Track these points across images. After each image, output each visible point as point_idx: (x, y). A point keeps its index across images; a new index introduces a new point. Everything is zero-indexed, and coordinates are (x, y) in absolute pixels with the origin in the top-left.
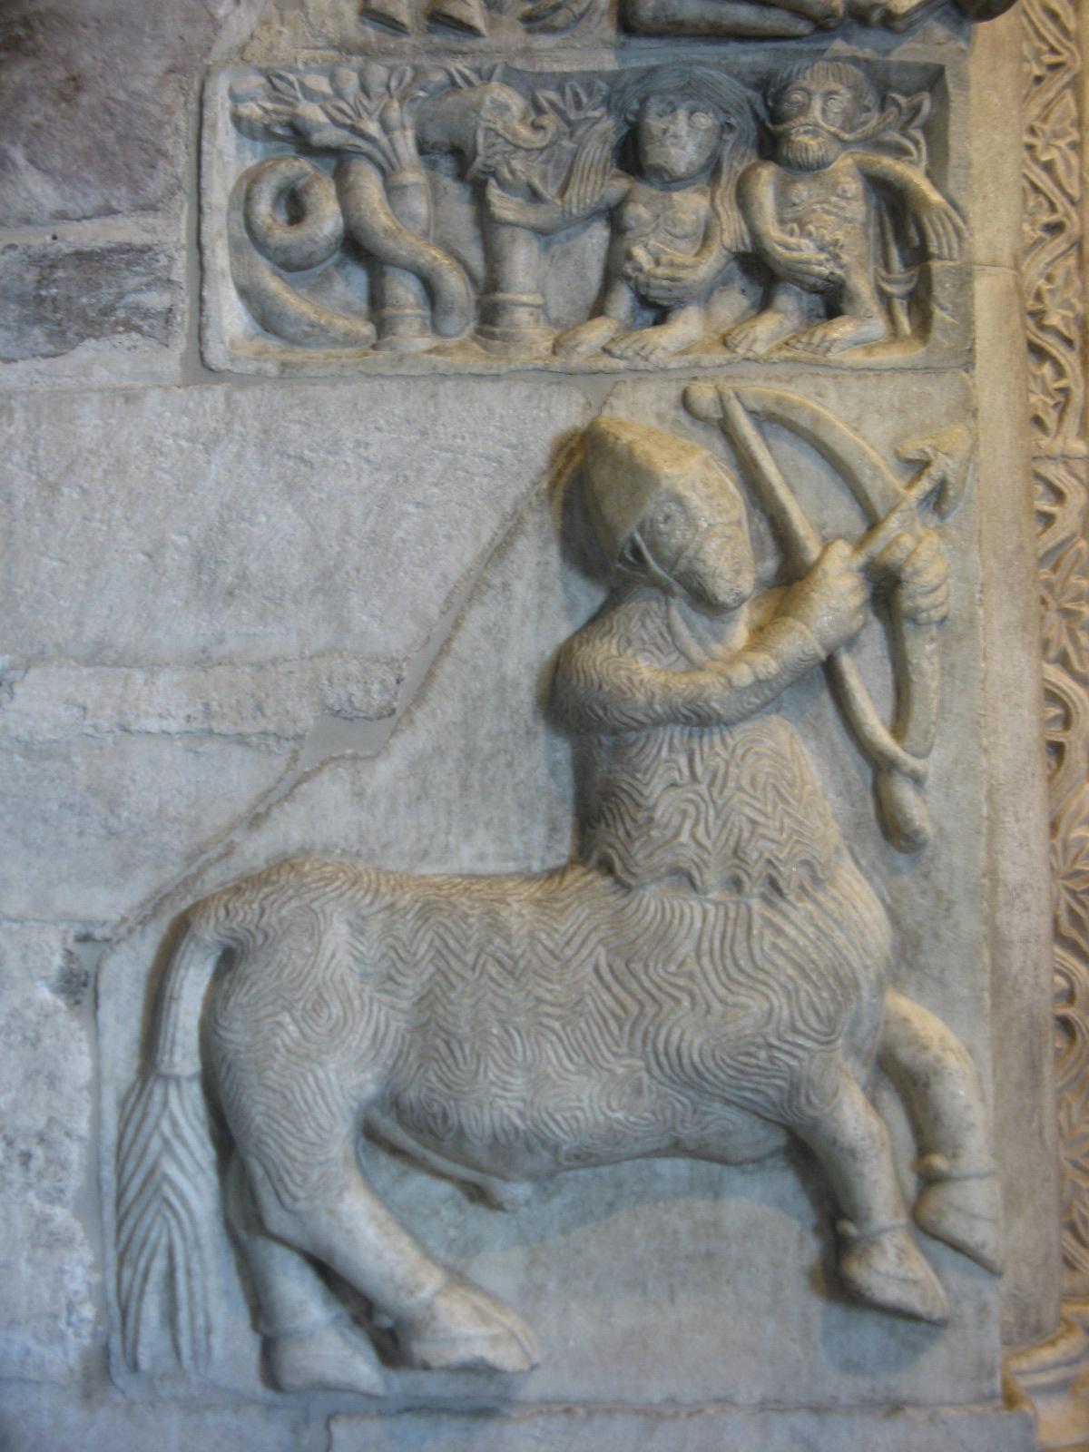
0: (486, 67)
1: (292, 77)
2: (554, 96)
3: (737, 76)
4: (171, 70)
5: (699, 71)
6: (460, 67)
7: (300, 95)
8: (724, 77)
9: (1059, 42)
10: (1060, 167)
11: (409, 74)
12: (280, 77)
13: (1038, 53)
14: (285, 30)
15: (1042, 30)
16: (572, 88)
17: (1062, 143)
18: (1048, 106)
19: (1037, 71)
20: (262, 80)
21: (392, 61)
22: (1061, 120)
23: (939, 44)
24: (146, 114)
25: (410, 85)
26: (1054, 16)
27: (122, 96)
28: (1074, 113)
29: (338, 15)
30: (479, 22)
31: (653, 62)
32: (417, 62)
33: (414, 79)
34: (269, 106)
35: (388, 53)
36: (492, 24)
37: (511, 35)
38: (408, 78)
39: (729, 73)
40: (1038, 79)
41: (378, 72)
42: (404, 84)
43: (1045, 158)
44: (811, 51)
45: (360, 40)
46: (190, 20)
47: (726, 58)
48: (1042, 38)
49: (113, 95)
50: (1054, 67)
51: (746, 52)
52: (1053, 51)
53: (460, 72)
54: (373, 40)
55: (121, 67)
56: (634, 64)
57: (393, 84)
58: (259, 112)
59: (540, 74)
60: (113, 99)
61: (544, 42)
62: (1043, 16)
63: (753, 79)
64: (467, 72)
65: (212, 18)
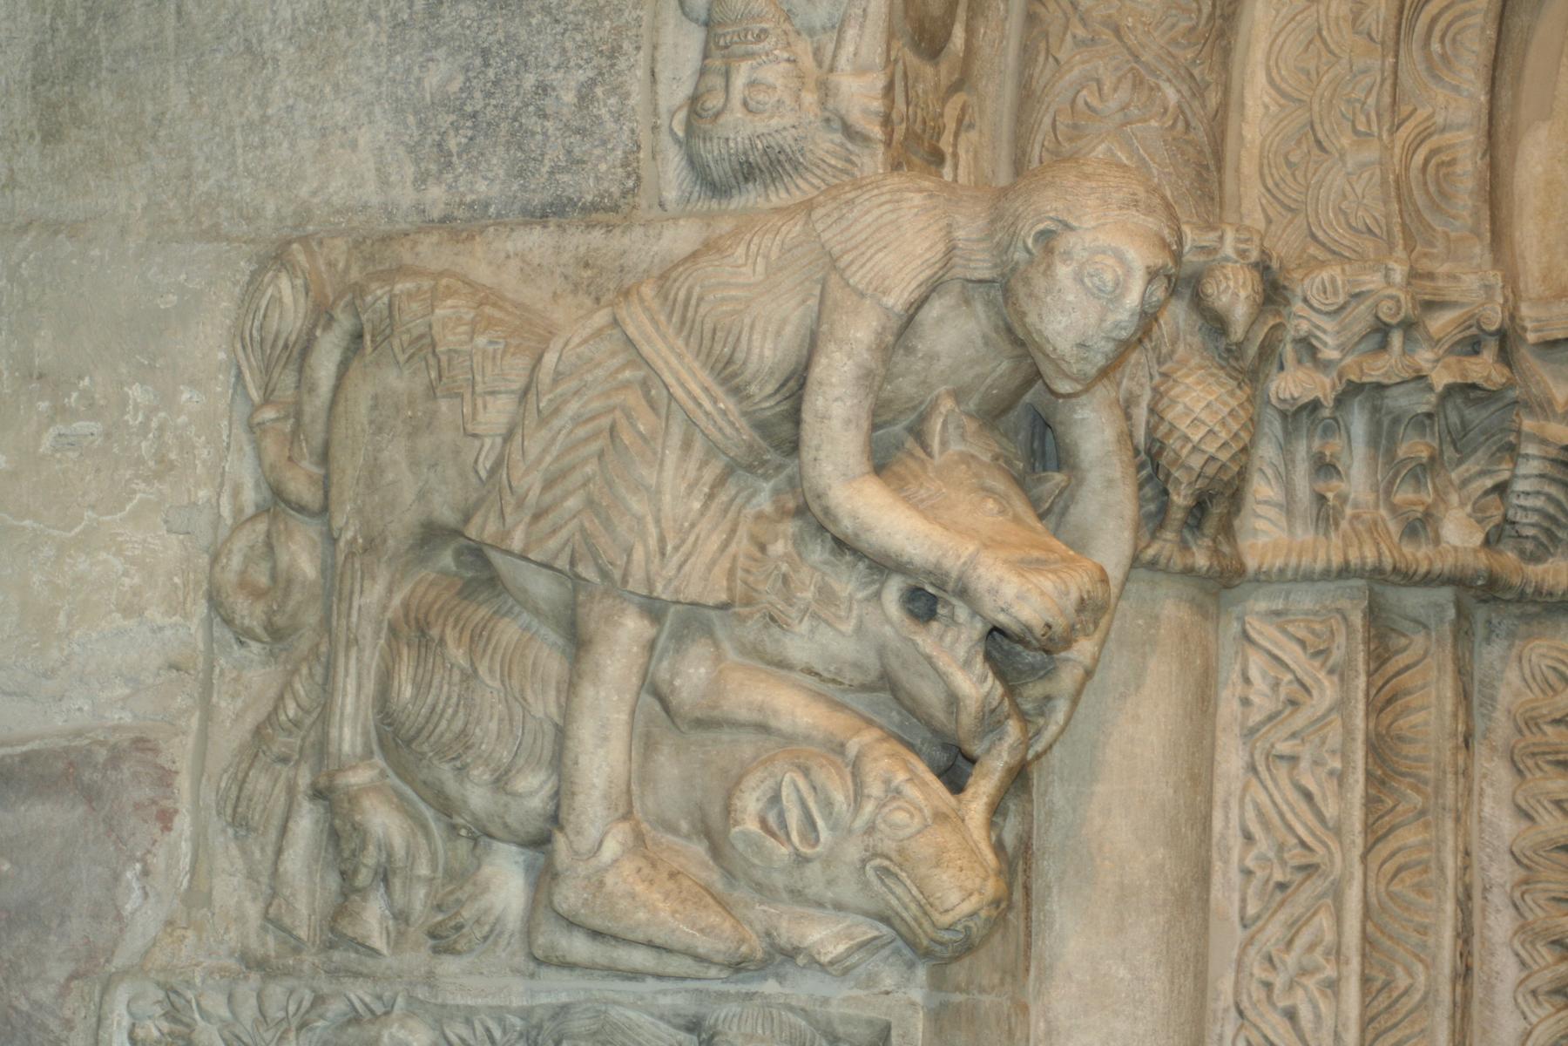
0: (387, 995)
1: (190, 995)
2: (464, 1032)
3: (661, 1017)
4: (74, 976)
5: (615, 1013)
6: (360, 993)
7: (197, 1016)
8: (645, 1019)
9: (1313, 834)
10: (1305, 1013)
11: (308, 997)
12: (176, 992)
13: (1281, 848)
14: (190, 933)
15: (1289, 816)
16: (482, 1023)
17: (1311, 983)
18: (1295, 927)
19: (1278, 876)
20: (161, 995)
21: (290, 982)
22: (1311, 947)
23: (887, 993)
24: (44, 1028)
25: (307, 1012)
26: (1308, 796)
27: (24, 1006)
28: (1329, 937)
29: (241, 919)
30: (378, 942)
31: (564, 998)
32: (315, 984)
33: (313, 1005)
34: (165, 1026)
35: (288, 973)
36: (397, 941)
37: (417, 958)
38: (306, 1004)
39: (652, 1015)
40: (1282, 886)
41: (276, 991)
42: (303, 1010)
43: (1283, 1003)
44: (738, 994)
45: (260, 952)
46: (96, 917)
47: (642, 998)
48: (1290, 828)
49: (15, 1003)
50: (1309, 869)
51: (664, 993)
52: (1303, 844)
53: (362, 1000)
54: (273, 954)
55: (25, 971)
56: (544, 999)
57: (292, 1009)
58: (156, 1034)
59: (444, 1006)
60: (15, 1008)
61: (449, 966)
62: (1294, 796)
63: (681, 1021)
64: (367, 999)
65: (119, 917)
